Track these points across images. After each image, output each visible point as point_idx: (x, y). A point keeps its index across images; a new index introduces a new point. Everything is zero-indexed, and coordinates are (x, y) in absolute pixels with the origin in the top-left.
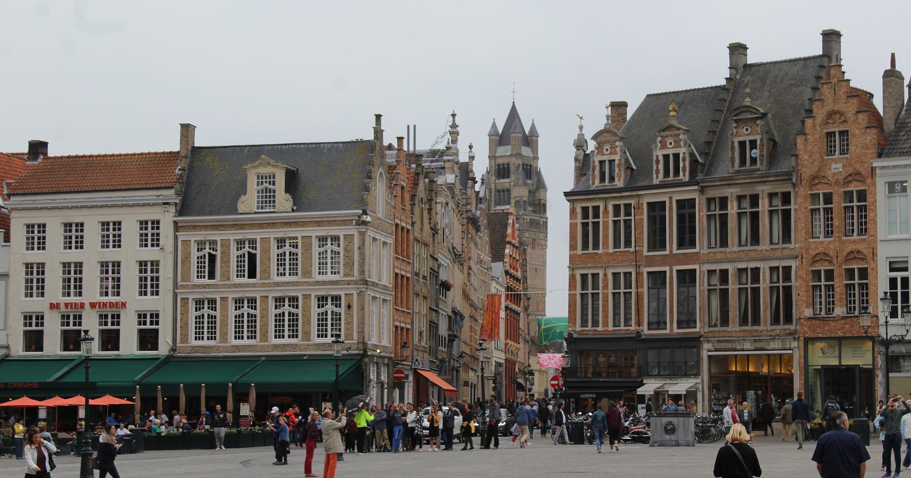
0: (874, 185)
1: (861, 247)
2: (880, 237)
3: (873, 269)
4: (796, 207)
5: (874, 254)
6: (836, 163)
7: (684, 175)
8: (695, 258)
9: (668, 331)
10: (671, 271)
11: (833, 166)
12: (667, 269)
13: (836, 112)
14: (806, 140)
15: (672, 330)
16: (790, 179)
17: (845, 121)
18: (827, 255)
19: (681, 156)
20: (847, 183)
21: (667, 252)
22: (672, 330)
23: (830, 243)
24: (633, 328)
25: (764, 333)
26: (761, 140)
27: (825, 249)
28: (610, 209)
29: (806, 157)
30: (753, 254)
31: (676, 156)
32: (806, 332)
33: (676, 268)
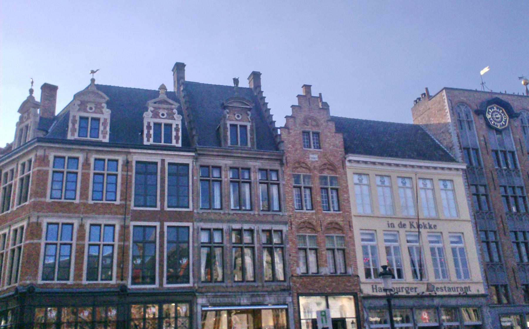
0: (345, 174)
1: (339, 220)
2: (353, 212)
3: (350, 237)
4: (284, 183)
5: (351, 226)
6: (313, 154)
7: (177, 142)
8: (189, 217)
9: (156, 286)
10: (162, 227)
11: (311, 156)
12: (157, 224)
13: (312, 118)
14: (289, 133)
15: (161, 284)
16: (281, 160)
17: (318, 125)
18: (310, 223)
19: (174, 126)
20: (321, 171)
21: (158, 209)
22: (161, 284)
23: (312, 214)
24: (114, 282)
25: (260, 288)
26: (252, 126)
27: (309, 218)
28: (92, 161)
29: (290, 146)
30: (247, 218)
31: (168, 126)
32: (298, 288)
33: (166, 224)
